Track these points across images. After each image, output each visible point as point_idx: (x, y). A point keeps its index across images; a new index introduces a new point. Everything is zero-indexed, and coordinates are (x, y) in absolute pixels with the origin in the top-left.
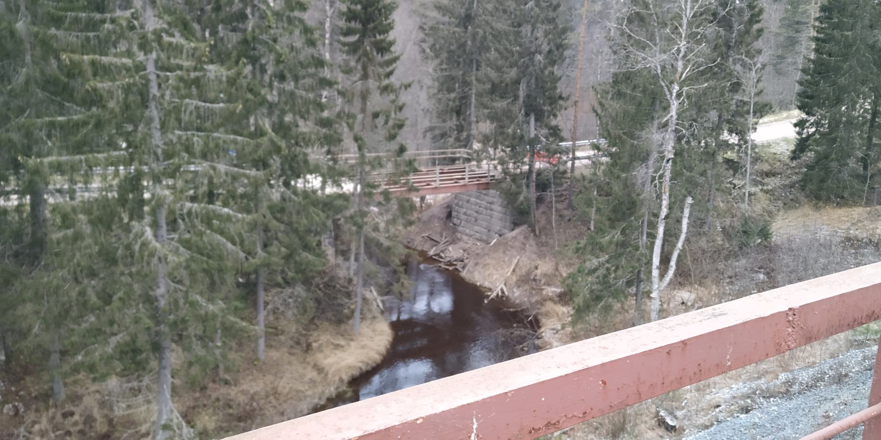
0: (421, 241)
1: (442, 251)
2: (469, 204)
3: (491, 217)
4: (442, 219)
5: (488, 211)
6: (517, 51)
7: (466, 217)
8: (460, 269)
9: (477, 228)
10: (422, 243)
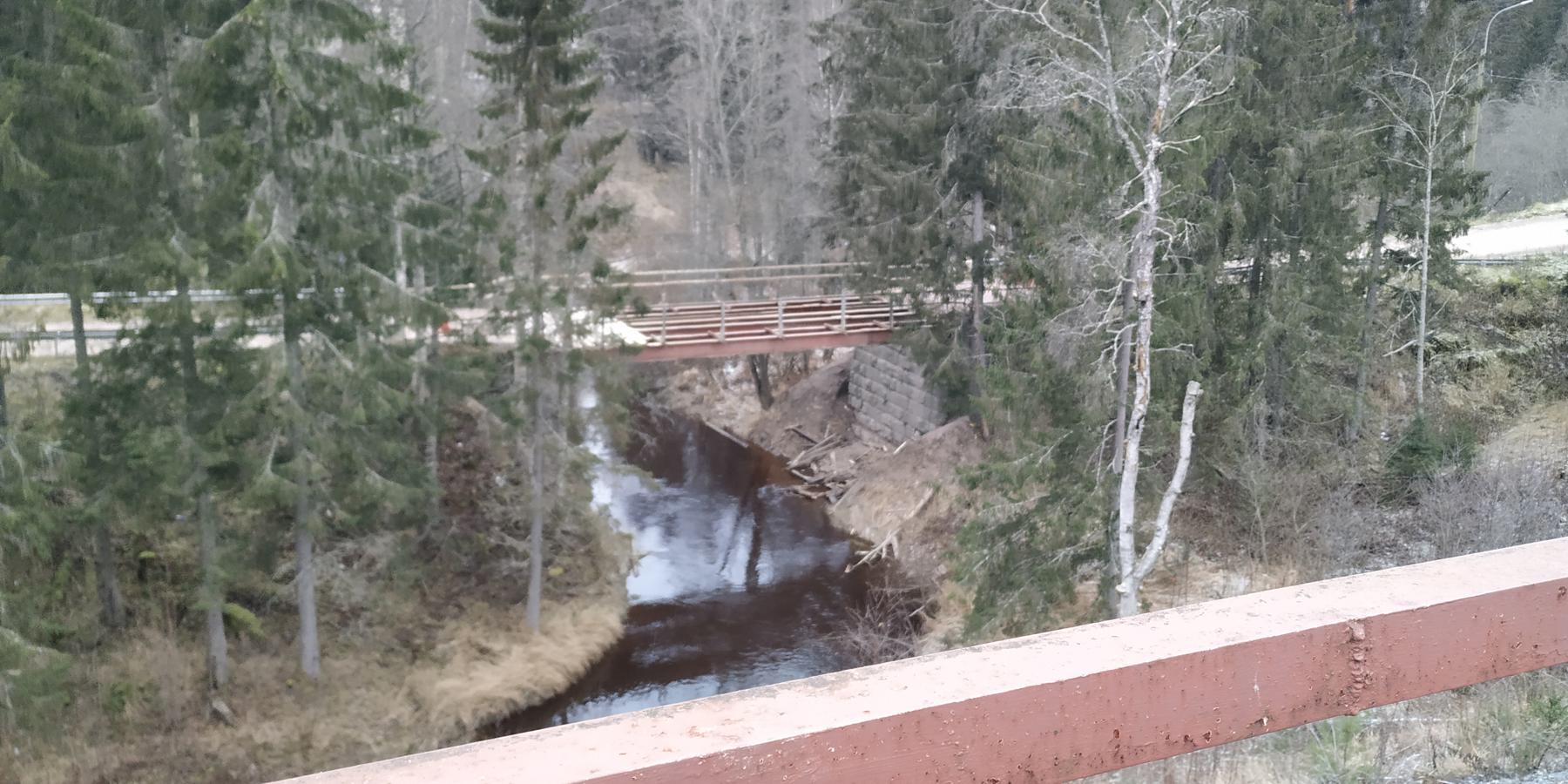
0: (783, 438)
1: (816, 461)
2: (875, 370)
3: (909, 397)
4: (830, 396)
5: (905, 385)
6: (935, 69)
8: (833, 499)
9: (886, 417)
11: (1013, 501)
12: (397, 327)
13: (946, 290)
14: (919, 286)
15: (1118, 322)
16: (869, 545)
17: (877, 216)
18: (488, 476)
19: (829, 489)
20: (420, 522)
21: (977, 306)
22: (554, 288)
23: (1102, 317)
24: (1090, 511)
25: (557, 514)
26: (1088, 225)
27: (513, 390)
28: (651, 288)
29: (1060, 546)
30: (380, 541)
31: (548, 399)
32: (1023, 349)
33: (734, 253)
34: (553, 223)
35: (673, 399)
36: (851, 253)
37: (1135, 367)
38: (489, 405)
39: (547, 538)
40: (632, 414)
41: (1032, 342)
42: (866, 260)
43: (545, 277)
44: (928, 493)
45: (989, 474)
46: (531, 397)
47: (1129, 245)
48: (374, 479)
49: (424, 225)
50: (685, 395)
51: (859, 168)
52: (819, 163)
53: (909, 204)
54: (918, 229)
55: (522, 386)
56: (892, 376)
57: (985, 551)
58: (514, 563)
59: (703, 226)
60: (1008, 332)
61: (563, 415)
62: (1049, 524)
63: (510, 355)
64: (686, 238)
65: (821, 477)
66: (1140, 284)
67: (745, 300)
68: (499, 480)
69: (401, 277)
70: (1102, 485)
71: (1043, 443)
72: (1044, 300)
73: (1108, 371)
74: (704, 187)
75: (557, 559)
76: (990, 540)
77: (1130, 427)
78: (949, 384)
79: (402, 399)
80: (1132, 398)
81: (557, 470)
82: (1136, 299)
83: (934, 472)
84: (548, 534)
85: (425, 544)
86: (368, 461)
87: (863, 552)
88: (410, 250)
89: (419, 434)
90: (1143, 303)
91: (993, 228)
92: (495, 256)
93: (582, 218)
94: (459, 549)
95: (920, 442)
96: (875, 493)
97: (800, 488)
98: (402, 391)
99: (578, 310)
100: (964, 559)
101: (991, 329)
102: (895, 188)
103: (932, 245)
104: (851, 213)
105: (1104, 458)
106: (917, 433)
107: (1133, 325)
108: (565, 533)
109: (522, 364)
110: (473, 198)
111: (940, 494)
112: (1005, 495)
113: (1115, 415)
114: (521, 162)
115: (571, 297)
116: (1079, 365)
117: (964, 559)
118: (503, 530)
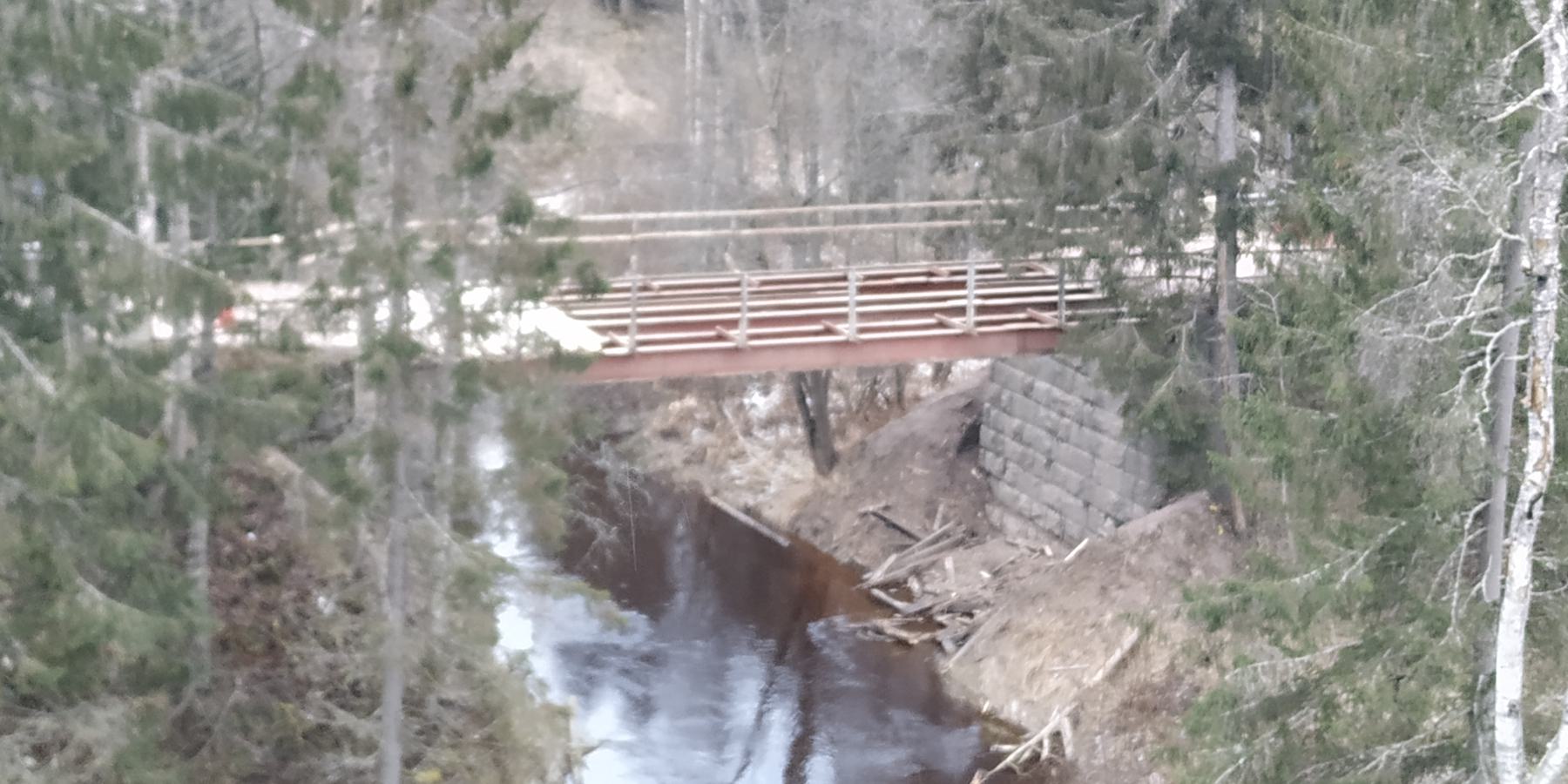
0: (855, 530)
3: (1095, 455)
5: (1087, 431)
7: (1020, 448)
8: (949, 646)
10: (856, 538)
11: (1292, 654)
12: (137, 317)
13: (1167, 252)
14: (1116, 244)
15: (1493, 316)
16: (1016, 733)
17: (1035, 113)
18: (304, 596)
19: (941, 626)
20: (175, 682)
21: (1224, 282)
22: (429, 246)
23: (1462, 306)
24: (1438, 675)
25: (430, 668)
26: (1437, 133)
27: (351, 435)
28: (611, 245)
29: (1382, 739)
30: (100, 715)
31: (416, 453)
32: (1310, 365)
33: (766, 181)
34: (430, 123)
35: (650, 453)
36: (986, 182)
37: (1526, 402)
38: (311, 465)
39: (412, 714)
40: (572, 483)
41: (1329, 352)
42: (1015, 196)
43: (413, 224)
44: (1131, 636)
45: (1247, 601)
46: (385, 448)
47: (1515, 170)
48: (93, 599)
49: (190, 127)
50: (673, 447)
51: (1003, 22)
52: (928, 13)
53: (1096, 90)
54: (1115, 136)
55: (367, 428)
56: (1062, 414)
57: (1238, 748)
58: (349, 761)
59: (708, 129)
60: (1284, 333)
61: (444, 482)
62: (1360, 697)
63: (346, 369)
64: (676, 153)
65: (927, 602)
66: (1536, 244)
67: (785, 268)
68: (324, 603)
69: (147, 224)
70: (1462, 623)
71: (1349, 545)
72: (1351, 272)
73: (1473, 408)
74: (710, 57)
75: (430, 753)
76: (1245, 726)
77: (1516, 514)
78: (1170, 428)
79: (146, 450)
80: (1519, 460)
81: (430, 587)
82: (1528, 273)
83: (1140, 596)
84: (413, 704)
85: (185, 722)
86: (80, 566)
87: (1006, 748)
88: (164, 172)
89: (175, 516)
90: (1542, 280)
91: (1256, 136)
92: (321, 184)
93: (484, 116)
94: (246, 731)
95: (1114, 540)
96: (1029, 635)
97: (888, 626)
98: (144, 434)
99: (475, 285)
100: (1196, 763)
101: (1251, 326)
102: (1070, 61)
103: (1140, 168)
104: (986, 106)
105: (1466, 574)
106: (1109, 522)
107: (1521, 322)
108: (443, 703)
109: (367, 387)
110: (280, 77)
111: (1153, 638)
112: (1276, 642)
113: (1487, 491)
114: (370, 11)
115: (461, 262)
116: (1418, 396)
117: (1196, 763)
118: (329, 697)
